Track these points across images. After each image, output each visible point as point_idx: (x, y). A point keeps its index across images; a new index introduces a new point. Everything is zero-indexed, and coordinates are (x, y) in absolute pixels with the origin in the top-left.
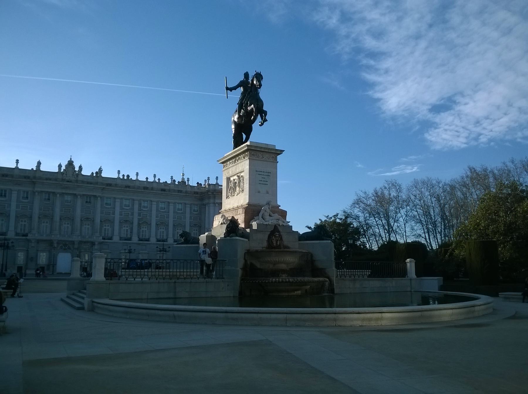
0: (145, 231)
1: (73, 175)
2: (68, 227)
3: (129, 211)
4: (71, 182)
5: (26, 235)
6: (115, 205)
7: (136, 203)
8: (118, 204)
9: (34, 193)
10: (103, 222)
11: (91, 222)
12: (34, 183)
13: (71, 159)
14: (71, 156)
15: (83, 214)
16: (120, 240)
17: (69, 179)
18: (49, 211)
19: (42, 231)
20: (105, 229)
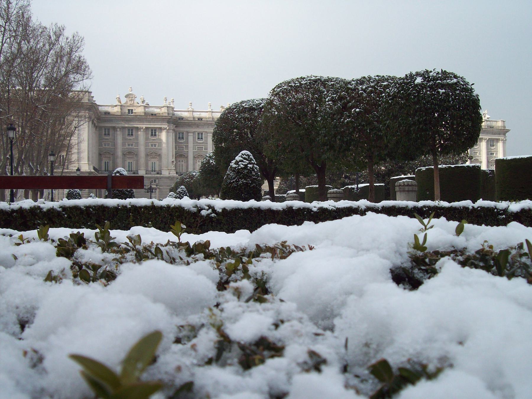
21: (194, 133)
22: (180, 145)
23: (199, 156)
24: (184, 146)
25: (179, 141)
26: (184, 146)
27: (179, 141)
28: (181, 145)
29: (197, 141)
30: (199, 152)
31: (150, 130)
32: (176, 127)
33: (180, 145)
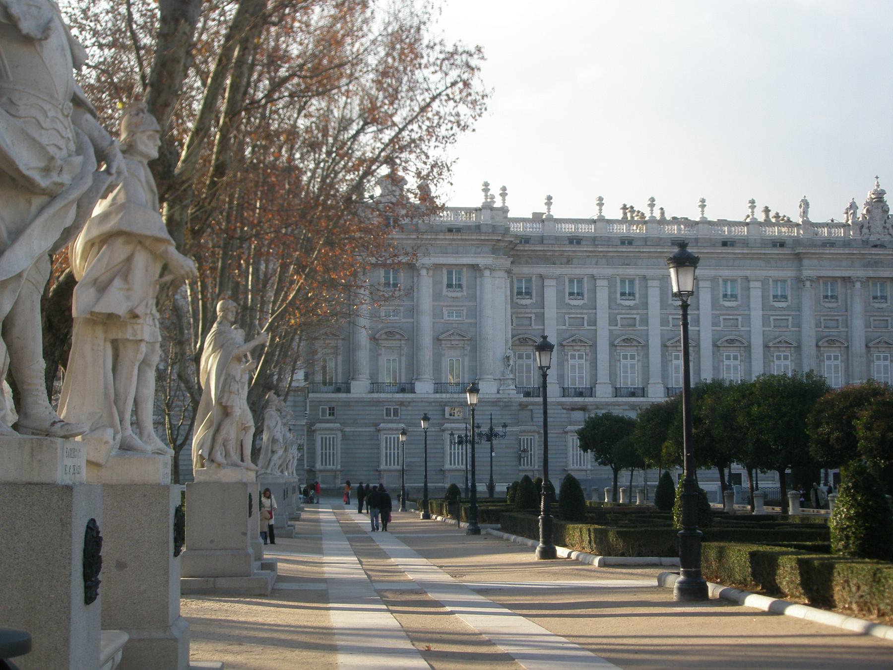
0: (886, 366)
1: (884, 227)
2: (886, 366)
4: (882, 246)
7: (756, 285)
9: (799, 280)
10: (670, 348)
12: (798, 257)
13: (878, 186)
14: (877, 178)
21: (558, 278)
22: (521, 313)
23: (573, 341)
24: (533, 317)
25: (518, 301)
26: (533, 317)
27: (518, 301)
28: (527, 313)
29: (567, 301)
30: (573, 332)
31: (445, 271)
32: (512, 263)
33: (521, 313)
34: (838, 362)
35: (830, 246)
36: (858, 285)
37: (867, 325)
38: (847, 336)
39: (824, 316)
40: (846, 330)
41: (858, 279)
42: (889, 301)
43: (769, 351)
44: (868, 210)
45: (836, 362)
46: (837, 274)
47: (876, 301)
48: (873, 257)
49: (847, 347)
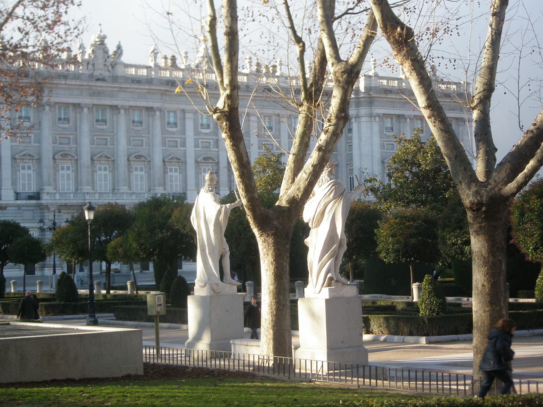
0: (106, 175)
1: (105, 65)
2: (106, 176)
3: (211, 137)
4: (103, 80)
5: (37, 196)
6: (279, 130)
8: (190, 125)
11: (146, 163)
13: (101, 32)
15: (130, 147)
16: (17, 199)
17: (101, 74)
18: (69, 144)
19: (60, 185)
20: (171, 176)
34: (70, 172)
35: (64, 78)
36: (86, 110)
37: (92, 143)
38: (76, 151)
39: (59, 134)
40: (75, 146)
41: (86, 105)
42: (108, 124)
43: (16, 162)
44: (93, 51)
45: (69, 172)
46: (70, 101)
47: (99, 123)
48: (98, 88)
49: (77, 160)
